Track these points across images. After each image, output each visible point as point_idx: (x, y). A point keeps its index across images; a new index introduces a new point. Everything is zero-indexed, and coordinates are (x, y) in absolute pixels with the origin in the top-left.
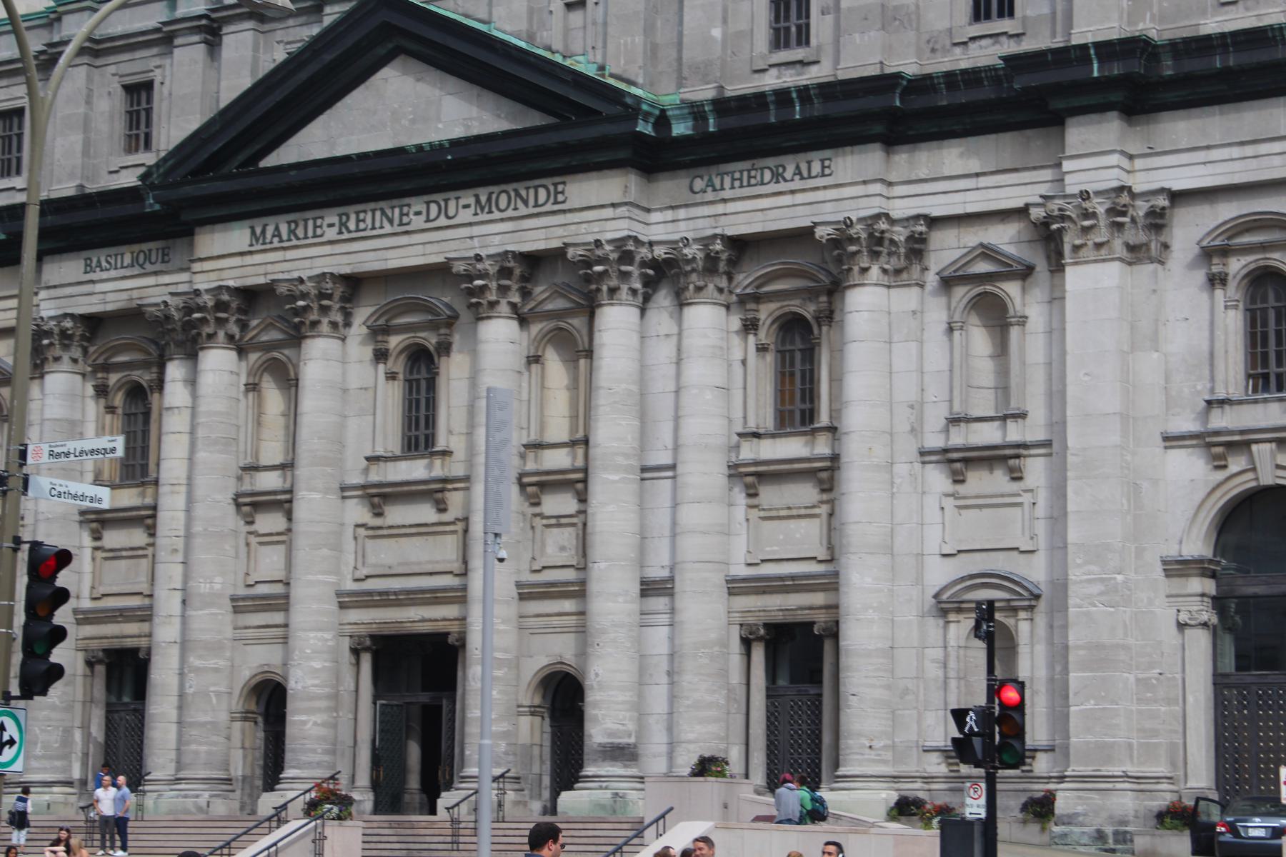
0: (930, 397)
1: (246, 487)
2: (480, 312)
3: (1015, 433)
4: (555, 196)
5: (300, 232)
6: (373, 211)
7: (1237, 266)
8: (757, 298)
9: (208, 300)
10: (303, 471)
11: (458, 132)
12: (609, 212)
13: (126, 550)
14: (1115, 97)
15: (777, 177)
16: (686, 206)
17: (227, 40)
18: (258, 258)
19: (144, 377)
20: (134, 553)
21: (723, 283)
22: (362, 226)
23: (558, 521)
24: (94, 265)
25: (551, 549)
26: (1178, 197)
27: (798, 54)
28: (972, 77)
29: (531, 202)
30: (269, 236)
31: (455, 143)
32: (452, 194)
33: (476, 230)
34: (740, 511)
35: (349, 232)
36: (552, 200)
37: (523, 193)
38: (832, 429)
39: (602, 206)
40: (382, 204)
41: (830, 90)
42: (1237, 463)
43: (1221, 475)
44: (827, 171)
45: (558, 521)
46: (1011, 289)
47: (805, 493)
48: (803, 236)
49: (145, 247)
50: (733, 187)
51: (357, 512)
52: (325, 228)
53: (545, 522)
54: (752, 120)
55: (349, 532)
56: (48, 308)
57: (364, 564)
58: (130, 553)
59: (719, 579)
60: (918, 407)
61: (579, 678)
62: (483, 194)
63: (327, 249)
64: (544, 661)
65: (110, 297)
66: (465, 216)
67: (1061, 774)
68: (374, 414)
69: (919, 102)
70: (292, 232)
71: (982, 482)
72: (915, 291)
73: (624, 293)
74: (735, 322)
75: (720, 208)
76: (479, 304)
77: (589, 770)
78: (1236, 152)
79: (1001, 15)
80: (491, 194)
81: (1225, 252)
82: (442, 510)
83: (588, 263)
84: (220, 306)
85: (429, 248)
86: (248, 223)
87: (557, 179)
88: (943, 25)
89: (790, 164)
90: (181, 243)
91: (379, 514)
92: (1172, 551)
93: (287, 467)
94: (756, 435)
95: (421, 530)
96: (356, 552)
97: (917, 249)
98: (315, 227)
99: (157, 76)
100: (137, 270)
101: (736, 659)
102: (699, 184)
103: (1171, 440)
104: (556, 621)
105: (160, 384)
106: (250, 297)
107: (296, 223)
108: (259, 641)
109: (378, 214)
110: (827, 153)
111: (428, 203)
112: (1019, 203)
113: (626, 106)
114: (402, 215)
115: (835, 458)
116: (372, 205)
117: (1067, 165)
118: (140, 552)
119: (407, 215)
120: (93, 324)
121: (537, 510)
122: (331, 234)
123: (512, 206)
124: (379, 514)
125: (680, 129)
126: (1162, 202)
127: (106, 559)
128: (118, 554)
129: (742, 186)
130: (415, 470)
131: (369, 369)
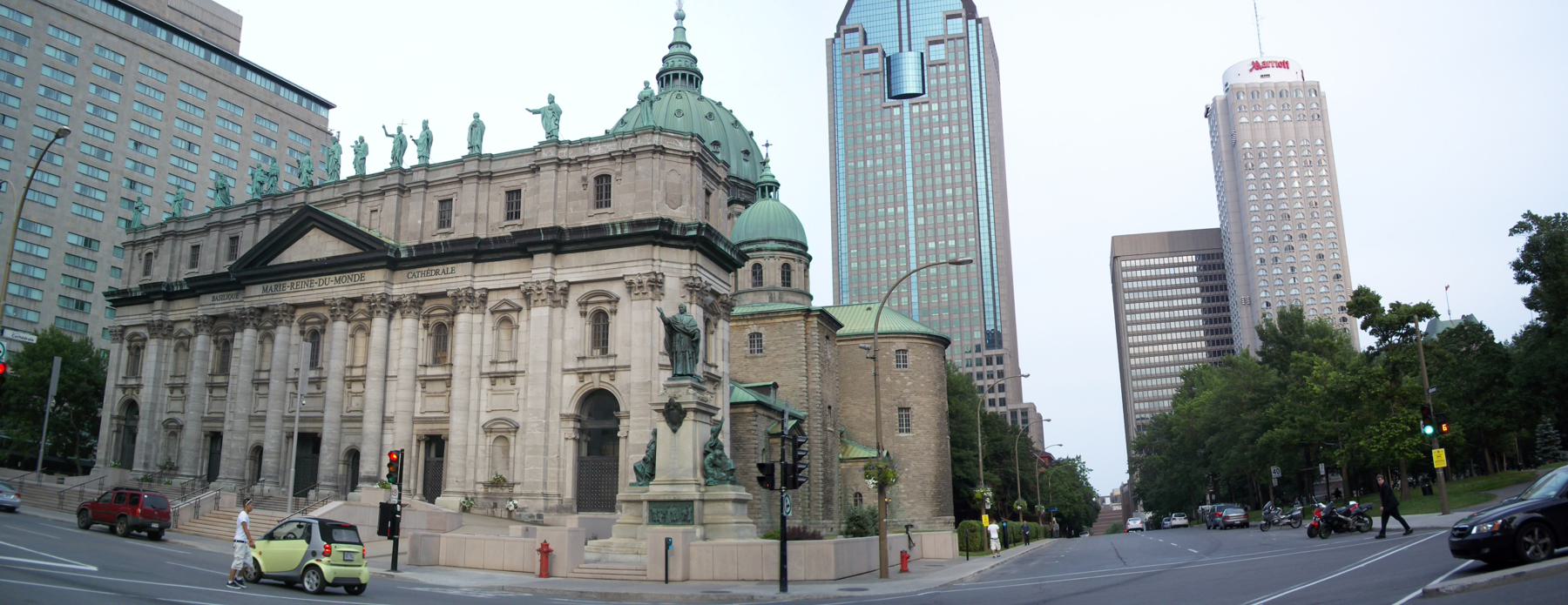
0: (485, 354)
1: (256, 377)
2: (335, 318)
3: (511, 368)
4: (361, 277)
7: (590, 309)
8: (429, 317)
9: (247, 311)
10: (273, 373)
11: (330, 255)
12: (378, 284)
14: (550, 247)
15: (437, 273)
17: (262, 223)
18: (265, 298)
19: (229, 337)
21: (417, 311)
23: (357, 394)
25: (353, 404)
26: (570, 284)
27: (447, 230)
28: (502, 239)
31: (328, 258)
33: (335, 290)
34: (419, 394)
38: (451, 365)
40: (306, 280)
41: (454, 243)
42: (588, 379)
43: (582, 384)
45: (357, 394)
46: (514, 315)
47: (440, 387)
48: (443, 295)
56: (200, 314)
59: (409, 417)
60: (481, 358)
62: (338, 276)
66: (332, 284)
67: (529, 491)
69: (483, 248)
71: (503, 385)
72: (481, 316)
73: (382, 313)
74: (421, 326)
75: (416, 284)
77: (359, 485)
78: (590, 268)
79: (516, 218)
81: (586, 304)
82: (319, 388)
83: (369, 301)
84: (251, 313)
88: (497, 220)
89: (441, 268)
90: (241, 292)
92: (564, 411)
93: (269, 371)
94: (426, 366)
97: (484, 300)
101: (414, 448)
102: (410, 275)
103: (566, 371)
105: (233, 340)
106: (263, 310)
112: (517, 285)
115: (451, 375)
117: (533, 272)
120: (215, 318)
125: (404, 255)
126: (565, 285)
131: (299, 336)
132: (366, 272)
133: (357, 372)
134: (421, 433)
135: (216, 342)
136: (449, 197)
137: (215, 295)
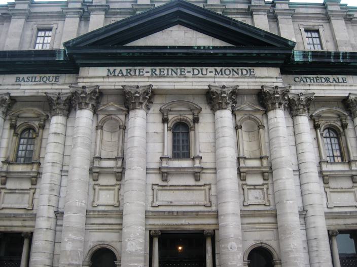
5: (132, 73)
6: (168, 70)
12: (274, 80)
13: (18, 190)
15: (327, 80)
16: (295, 85)
20: (23, 192)
22: (162, 73)
24: (21, 79)
25: (250, 198)
29: (240, 73)
30: (117, 73)
32: (204, 68)
33: (217, 80)
35: (156, 75)
36: (249, 73)
37: (236, 71)
39: (272, 77)
40: (174, 68)
44: (345, 81)
45: (255, 187)
49: (47, 75)
50: (311, 82)
51: (156, 179)
52: (144, 72)
53: (248, 187)
54: (326, 60)
55: (150, 187)
57: (157, 200)
58: (20, 191)
61: (249, 252)
62: (219, 69)
63: (146, 80)
64: (253, 243)
65: (26, 91)
66: (213, 74)
68: (163, 142)
70: (127, 72)
76: (221, 103)
80: (221, 70)
82: (197, 180)
85: (194, 84)
86: (108, 68)
87: (250, 68)
89: (331, 77)
91: (165, 180)
95: (187, 188)
96: (153, 195)
98: (140, 72)
99: (55, 27)
100: (42, 82)
102: (297, 80)
104: (257, 226)
107: (131, 70)
108: (100, 230)
109: (170, 71)
110: (343, 76)
111: (193, 70)
113: (288, 45)
114: (181, 72)
116: (167, 68)
118: (26, 191)
119: (184, 72)
120: (13, 100)
121: (244, 182)
122: (149, 74)
123: (232, 74)
124: (165, 180)
125: (298, 59)
127: (5, 193)
128: (14, 191)
129: (314, 82)
130: (185, 163)
132: (255, 68)
133: (256, 163)
134: (332, 228)
135: (13, 127)
136: (316, 28)
137: (21, 76)
